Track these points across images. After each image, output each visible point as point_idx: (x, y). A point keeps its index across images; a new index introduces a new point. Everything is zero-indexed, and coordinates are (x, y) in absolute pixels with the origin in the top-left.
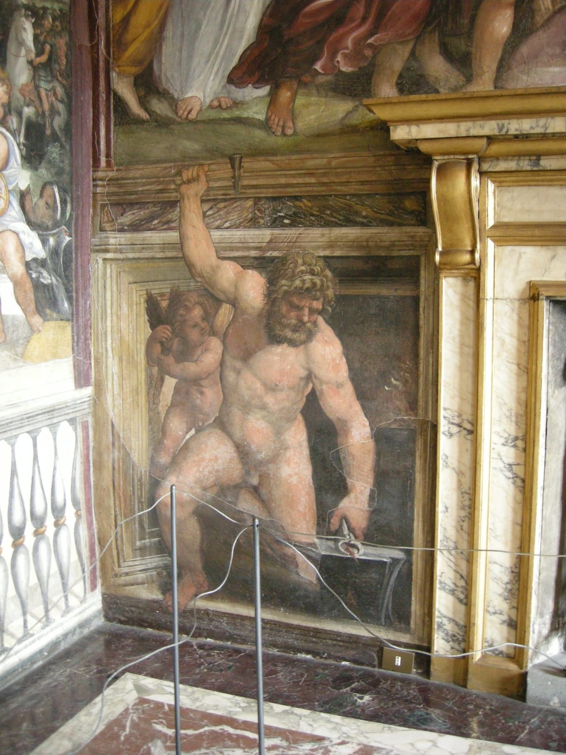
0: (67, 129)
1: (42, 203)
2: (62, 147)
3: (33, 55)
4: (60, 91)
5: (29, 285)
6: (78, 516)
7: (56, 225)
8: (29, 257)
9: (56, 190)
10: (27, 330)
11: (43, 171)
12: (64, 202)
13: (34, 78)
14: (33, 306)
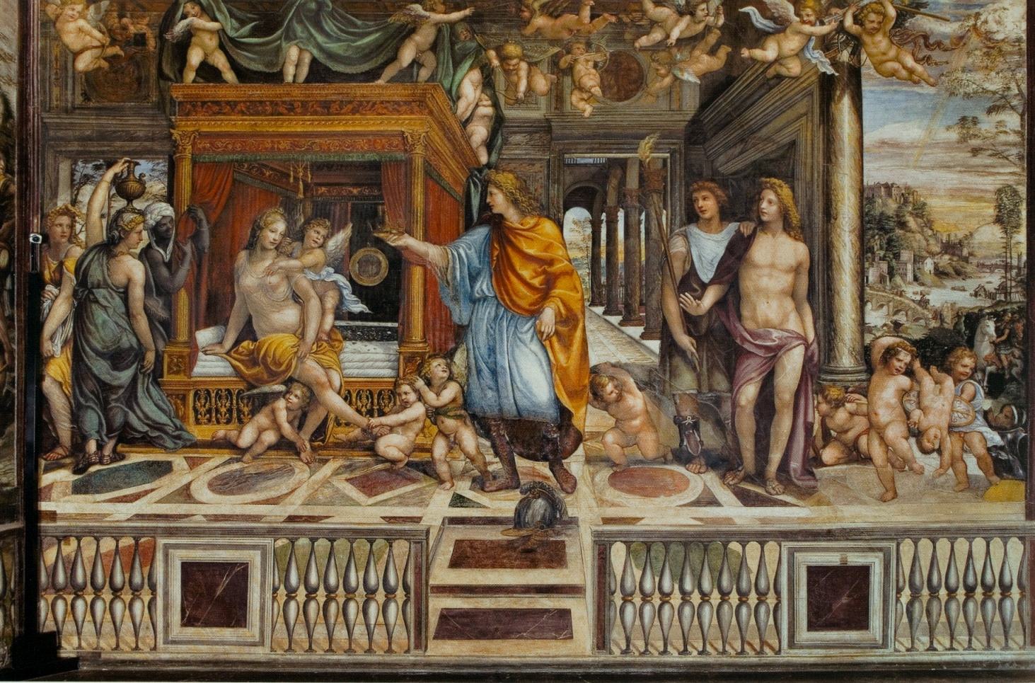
0: (1024, 373)
1: (1001, 416)
2: (1019, 383)
3: (994, 339)
4: (1017, 353)
5: (989, 460)
6: (1023, 596)
7: (1013, 427)
8: (990, 445)
9: (1013, 408)
10: (986, 483)
11: (1003, 400)
12: (1020, 415)
13: (995, 350)
14: (992, 471)
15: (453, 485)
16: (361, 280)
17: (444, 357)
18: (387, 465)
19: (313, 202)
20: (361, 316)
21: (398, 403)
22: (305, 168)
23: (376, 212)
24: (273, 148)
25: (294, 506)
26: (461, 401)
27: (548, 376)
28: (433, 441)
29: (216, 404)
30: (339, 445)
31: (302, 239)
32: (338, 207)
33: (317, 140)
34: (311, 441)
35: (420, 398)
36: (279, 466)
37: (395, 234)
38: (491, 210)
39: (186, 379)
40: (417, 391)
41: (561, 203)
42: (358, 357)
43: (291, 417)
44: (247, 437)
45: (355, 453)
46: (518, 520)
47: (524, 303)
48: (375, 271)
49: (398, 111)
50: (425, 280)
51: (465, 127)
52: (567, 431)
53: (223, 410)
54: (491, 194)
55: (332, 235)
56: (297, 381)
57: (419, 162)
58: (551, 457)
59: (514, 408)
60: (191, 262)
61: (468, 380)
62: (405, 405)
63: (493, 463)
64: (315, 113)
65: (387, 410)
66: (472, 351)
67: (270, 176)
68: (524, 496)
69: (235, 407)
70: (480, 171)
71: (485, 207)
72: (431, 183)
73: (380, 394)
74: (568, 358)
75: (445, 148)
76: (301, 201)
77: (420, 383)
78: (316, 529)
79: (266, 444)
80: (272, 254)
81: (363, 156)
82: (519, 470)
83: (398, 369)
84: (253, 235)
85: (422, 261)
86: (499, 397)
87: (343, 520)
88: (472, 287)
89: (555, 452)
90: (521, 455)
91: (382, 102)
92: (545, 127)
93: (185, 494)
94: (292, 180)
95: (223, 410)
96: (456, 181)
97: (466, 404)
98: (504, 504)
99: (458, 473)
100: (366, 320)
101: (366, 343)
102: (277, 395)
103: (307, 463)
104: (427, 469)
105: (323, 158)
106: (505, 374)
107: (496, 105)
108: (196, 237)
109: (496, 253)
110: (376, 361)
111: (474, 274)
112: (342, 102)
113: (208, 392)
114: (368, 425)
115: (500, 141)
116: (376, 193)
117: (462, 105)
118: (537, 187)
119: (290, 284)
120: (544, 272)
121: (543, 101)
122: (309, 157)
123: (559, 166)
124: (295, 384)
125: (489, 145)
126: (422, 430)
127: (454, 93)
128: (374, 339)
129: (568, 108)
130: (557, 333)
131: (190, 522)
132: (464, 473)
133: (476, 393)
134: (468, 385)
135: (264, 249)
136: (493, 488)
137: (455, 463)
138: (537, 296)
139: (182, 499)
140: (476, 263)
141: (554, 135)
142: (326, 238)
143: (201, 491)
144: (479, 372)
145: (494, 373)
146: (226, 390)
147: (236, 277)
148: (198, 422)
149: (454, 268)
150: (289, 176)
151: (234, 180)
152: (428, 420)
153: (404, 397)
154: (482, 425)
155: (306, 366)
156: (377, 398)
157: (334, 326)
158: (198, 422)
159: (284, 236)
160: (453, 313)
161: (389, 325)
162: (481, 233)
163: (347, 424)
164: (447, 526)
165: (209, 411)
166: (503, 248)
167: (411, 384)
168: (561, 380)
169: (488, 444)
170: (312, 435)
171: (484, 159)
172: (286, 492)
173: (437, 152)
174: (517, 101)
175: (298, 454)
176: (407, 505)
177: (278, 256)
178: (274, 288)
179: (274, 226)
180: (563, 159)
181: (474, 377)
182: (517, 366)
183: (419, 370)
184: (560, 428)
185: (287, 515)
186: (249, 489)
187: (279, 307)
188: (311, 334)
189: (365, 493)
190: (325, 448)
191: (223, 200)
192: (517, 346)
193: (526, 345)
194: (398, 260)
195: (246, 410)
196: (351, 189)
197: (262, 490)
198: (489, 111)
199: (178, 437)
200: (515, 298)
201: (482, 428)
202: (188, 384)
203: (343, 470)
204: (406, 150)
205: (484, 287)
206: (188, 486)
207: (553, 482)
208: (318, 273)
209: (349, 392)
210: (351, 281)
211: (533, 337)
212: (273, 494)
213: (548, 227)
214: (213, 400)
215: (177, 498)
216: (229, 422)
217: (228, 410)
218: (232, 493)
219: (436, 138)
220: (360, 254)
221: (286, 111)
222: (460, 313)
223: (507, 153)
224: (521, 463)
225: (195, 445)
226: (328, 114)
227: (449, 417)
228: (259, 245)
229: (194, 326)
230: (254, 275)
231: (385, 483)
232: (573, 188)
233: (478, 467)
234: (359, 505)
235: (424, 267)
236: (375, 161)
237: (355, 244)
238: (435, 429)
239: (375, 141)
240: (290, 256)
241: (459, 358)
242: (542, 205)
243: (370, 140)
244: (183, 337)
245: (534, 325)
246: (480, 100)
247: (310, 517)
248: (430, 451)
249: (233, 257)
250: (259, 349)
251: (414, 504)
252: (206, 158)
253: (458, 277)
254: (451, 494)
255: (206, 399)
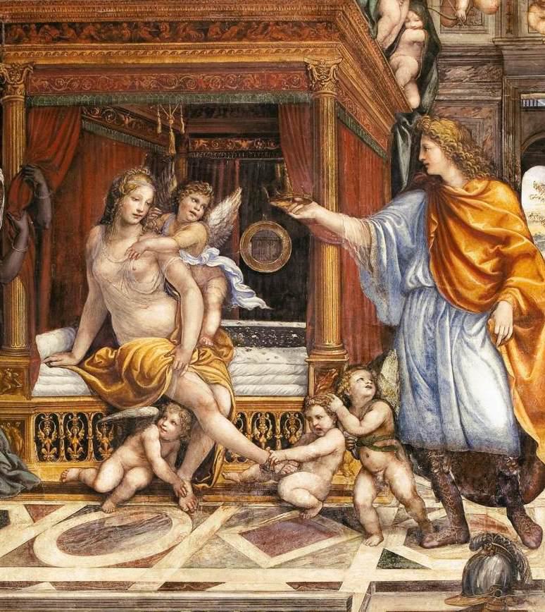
15: (382, 540)
16: (255, 264)
17: (369, 369)
18: (296, 513)
19: (188, 159)
20: (257, 314)
21: (309, 431)
22: (177, 114)
23: (273, 171)
24: (133, 86)
25: (172, 570)
26: (391, 426)
27: (506, 393)
28: (356, 481)
29: (66, 434)
30: (228, 487)
31: (175, 210)
32: (222, 166)
33: (191, 76)
34: (193, 482)
35: (338, 423)
36: (151, 516)
37: (299, 203)
38: (426, 170)
39: (24, 400)
40: (332, 414)
41: (519, 161)
42: (254, 368)
43: (166, 452)
44: (107, 478)
45: (253, 498)
46: (467, 586)
47: (471, 296)
48: (274, 251)
49: (300, 36)
50: (341, 265)
51: (388, 57)
52: (530, 466)
53: (75, 441)
54: (425, 149)
55: (216, 204)
56: (173, 401)
57: (328, 104)
58: (509, 501)
59: (461, 436)
60: (28, 243)
61: (400, 399)
62: (318, 434)
63: (432, 510)
64: (188, 38)
65: (293, 439)
66: (404, 361)
67: (130, 124)
68: (474, 553)
69: (90, 437)
70: (410, 117)
71: (418, 166)
72: (345, 134)
73: (284, 418)
74: (531, 369)
75: (363, 87)
76: (173, 158)
77: (337, 404)
78: (202, 600)
79: (134, 487)
80: (135, 231)
81: (253, 97)
82: (469, 518)
83: (308, 386)
84: (111, 204)
85: (336, 239)
86: (442, 422)
87: (239, 587)
88: (403, 274)
89: (515, 493)
90: (471, 498)
91: (277, 23)
92: (493, 57)
93: (27, 555)
94: (159, 130)
95: (75, 441)
96: (378, 131)
97: (398, 432)
98: (449, 564)
99: (388, 523)
100: (264, 318)
101: (264, 350)
102: (146, 421)
103: (189, 512)
104: (349, 520)
105: (200, 100)
106: (448, 391)
107: (428, 27)
108: (33, 208)
109: (434, 228)
110: (278, 374)
111: (406, 257)
112: (223, 22)
113: (55, 418)
114: (269, 460)
115: (435, 76)
116: (272, 147)
117: (384, 26)
118: (485, 137)
119: (160, 274)
120: (498, 253)
121: (491, 22)
122: (182, 98)
123: (514, 112)
124: (171, 405)
125: (421, 80)
126: (341, 466)
127: (372, 10)
128: (274, 345)
129: (524, 30)
130: (515, 335)
131: (34, 591)
132: (397, 522)
133: (411, 416)
134: (401, 406)
135: (125, 224)
136: (435, 543)
137: (383, 510)
138: (489, 286)
139: (22, 561)
140: (407, 240)
141: (507, 68)
142: (208, 208)
143: (48, 550)
144: (415, 388)
145: (435, 389)
146: (79, 414)
147: (88, 262)
148: (41, 458)
149: (379, 248)
150: (157, 125)
151: (83, 131)
152: (349, 453)
153: (316, 422)
154: (420, 459)
155: (185, 382)
156: (280, 425)
157: (220, 327)
158: (41, 458)
159: (151, 205)
160: (379, 308)
161: (295, 325)
162: (412, 202)
163: (241, 460)
164: (376, 593)
165: (56, 443)
166: (443, 223)
167: (325, 405)
168: (521, 398)
169: (428, 484)
170: (194, 475)
171: (414, 100)
172: (161, 550)
173: (352, 92)
174: (457, 21)
175: (176, 500)
176: (322, 567)
177: (144, 233)
178: (139, 276)
179: (137, 192)
180: (520, 101)
181: (409, 396)
182: (464, 380)
183: (334, 387)
184: (520, 462)
185: (163, 581)
186: (112, 547)
187: (145, 300)
188: (190, 339)
189: (266, 551)
190: (212, 491)
191: (69, 157)
192: (465, 354)
193: (475, 351)
194: (306, 239)
195: (105, 441)
196: (239, 142)
197: (129, 548)
198: (420, 35)
199: (16, 479)
200: (460, 289)
201: (419, 462)
202: (29, 406)
203: (236, 520)
204: (310, 89)
205: (420, 274)
206: (30, 544)
207: (512, 534)
208: (197, 256)
209: (243, 416)
210: (241, 265)
211: (484, 341)
212: (143, 553)
213: (501, 192)
214: (62, 428)
215: (16, 559)
216: (83, 457)
217: (82, 442)
218: (89, 552)
219: (351, 72)
220: (253, 229)
221: (149, 37)
222: (388, 310)
223: (446, 92)
224: (472, 510)
225: (40, 489)
226: (206, 40)
227: (375, 448)
228: (118, 219)
229: (33, 330)
230: (110, 259)
231: (291, 538)
232: (533, 140)
233: (414, 516)
234: (257, 566)
235: (340, 247)
236: (270, 105)
237: (244, 217)
238: (357, 466)
239: (269, 76)
240: (160, 232)
241: (388, 369)
242: (492, 163)
243: (262, 76)
244: (19, 344)
245: (486, 324)
246: (407, 20)
247: (193, 584)
248: (351, 494)
249: (83, 234)
250: (121, 358)
251: (332, 565)
252: (43, 100)
253: (385, 261)
254: (382, 549)
255: (53, 428)
